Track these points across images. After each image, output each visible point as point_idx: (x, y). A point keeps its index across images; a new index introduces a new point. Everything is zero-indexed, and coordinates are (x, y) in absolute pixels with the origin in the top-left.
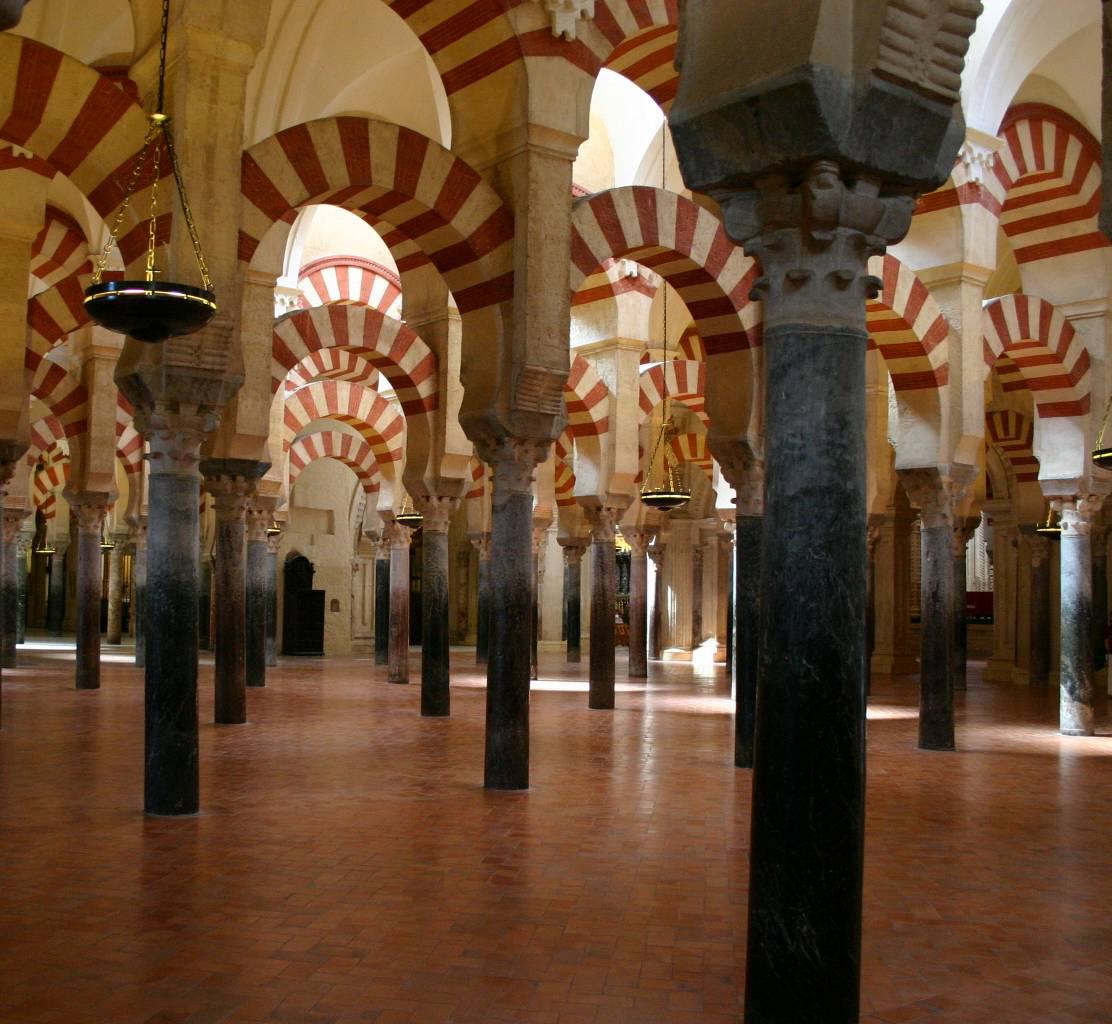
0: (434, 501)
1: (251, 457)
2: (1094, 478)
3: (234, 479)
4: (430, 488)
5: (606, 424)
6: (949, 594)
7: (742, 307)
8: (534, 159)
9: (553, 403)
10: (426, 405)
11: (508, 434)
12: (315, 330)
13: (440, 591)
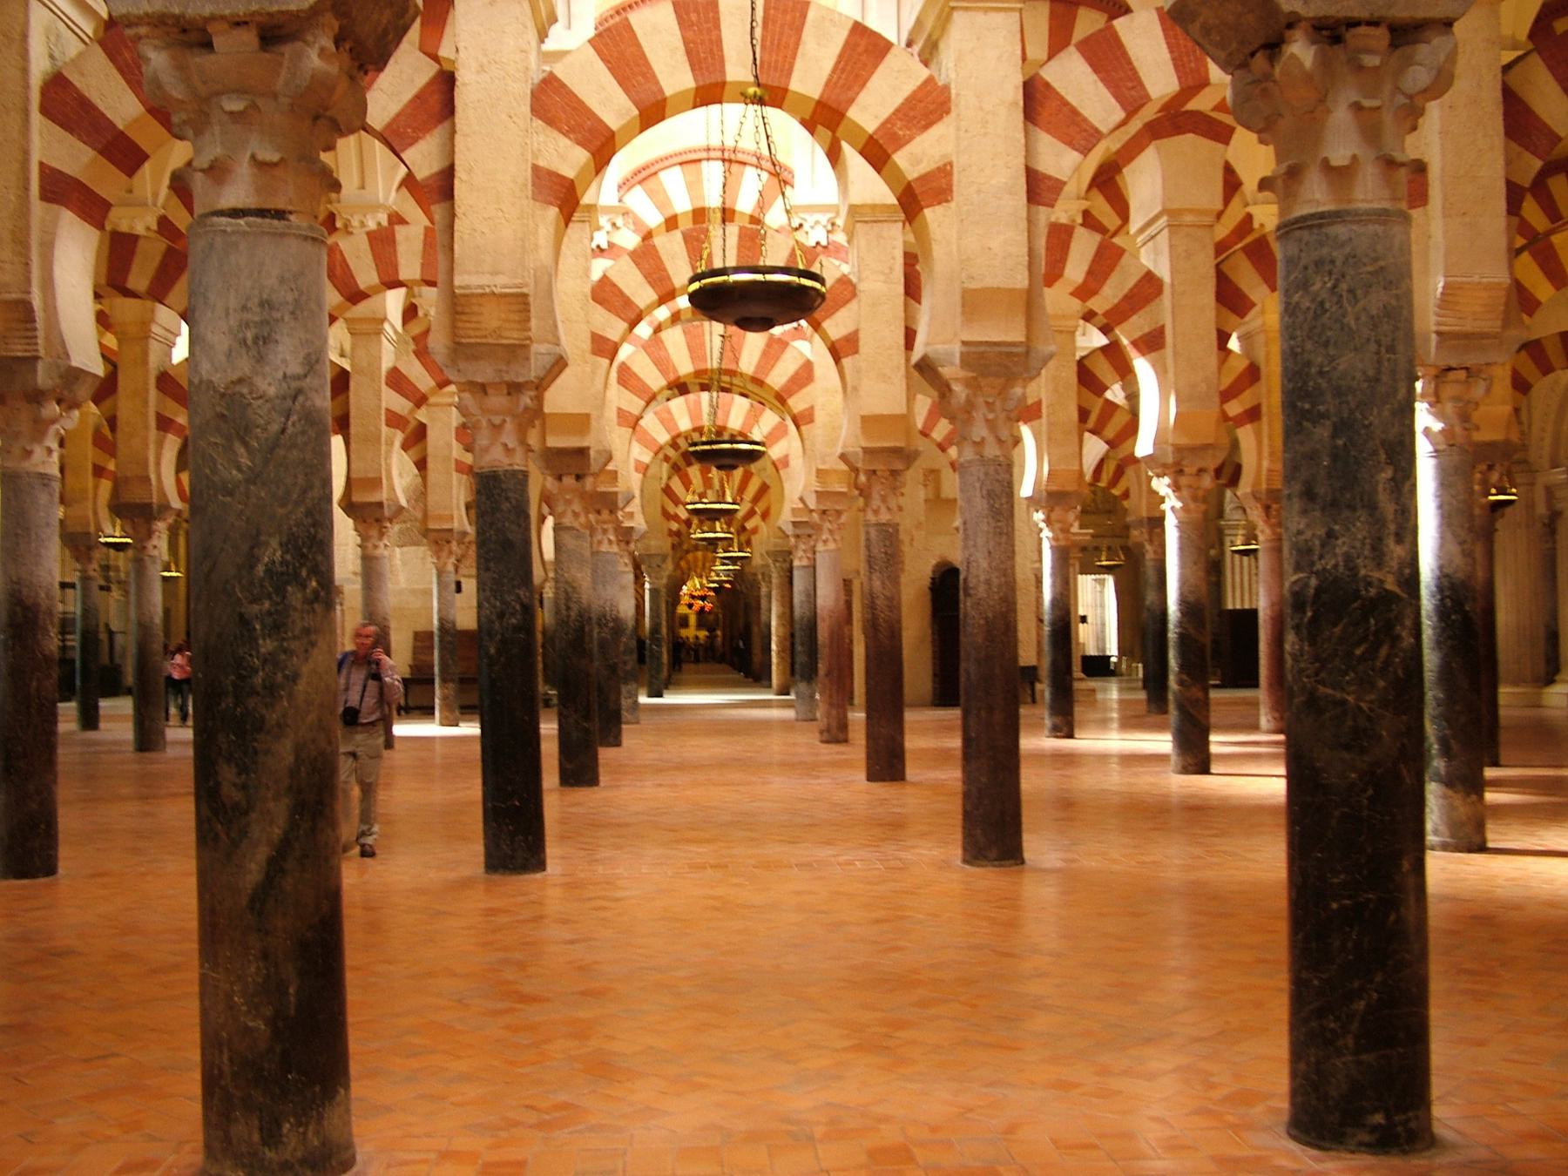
2: (1439, 333)
6: (988, 582)
7: (413, 141)
9: (23, 341)
12: (348, 266)
13: (568, 608)
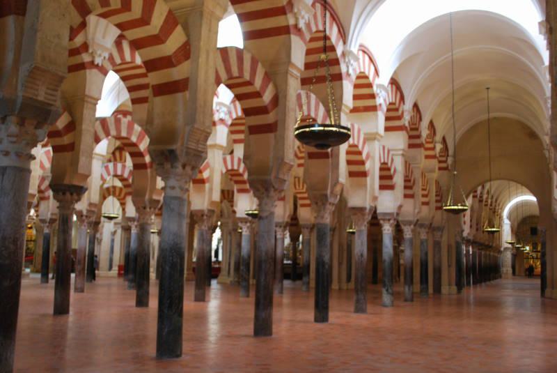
0: (148, 210)
1: (81, 185)
3: (72, 194)
4: (147, 203)
5: (209, 179)
8: (289, 76)
10: (148, 165)
11: (273, 187)
